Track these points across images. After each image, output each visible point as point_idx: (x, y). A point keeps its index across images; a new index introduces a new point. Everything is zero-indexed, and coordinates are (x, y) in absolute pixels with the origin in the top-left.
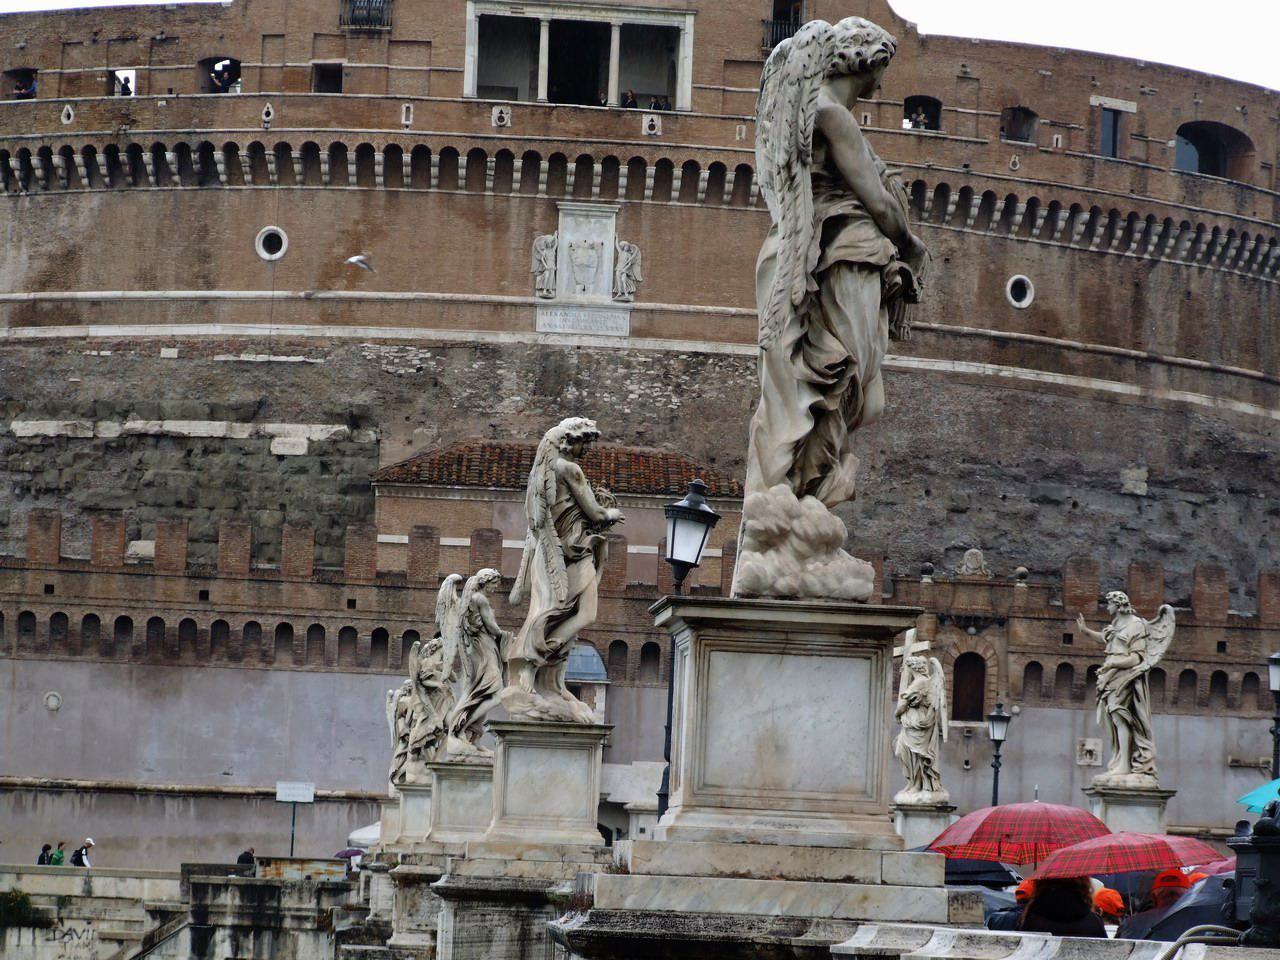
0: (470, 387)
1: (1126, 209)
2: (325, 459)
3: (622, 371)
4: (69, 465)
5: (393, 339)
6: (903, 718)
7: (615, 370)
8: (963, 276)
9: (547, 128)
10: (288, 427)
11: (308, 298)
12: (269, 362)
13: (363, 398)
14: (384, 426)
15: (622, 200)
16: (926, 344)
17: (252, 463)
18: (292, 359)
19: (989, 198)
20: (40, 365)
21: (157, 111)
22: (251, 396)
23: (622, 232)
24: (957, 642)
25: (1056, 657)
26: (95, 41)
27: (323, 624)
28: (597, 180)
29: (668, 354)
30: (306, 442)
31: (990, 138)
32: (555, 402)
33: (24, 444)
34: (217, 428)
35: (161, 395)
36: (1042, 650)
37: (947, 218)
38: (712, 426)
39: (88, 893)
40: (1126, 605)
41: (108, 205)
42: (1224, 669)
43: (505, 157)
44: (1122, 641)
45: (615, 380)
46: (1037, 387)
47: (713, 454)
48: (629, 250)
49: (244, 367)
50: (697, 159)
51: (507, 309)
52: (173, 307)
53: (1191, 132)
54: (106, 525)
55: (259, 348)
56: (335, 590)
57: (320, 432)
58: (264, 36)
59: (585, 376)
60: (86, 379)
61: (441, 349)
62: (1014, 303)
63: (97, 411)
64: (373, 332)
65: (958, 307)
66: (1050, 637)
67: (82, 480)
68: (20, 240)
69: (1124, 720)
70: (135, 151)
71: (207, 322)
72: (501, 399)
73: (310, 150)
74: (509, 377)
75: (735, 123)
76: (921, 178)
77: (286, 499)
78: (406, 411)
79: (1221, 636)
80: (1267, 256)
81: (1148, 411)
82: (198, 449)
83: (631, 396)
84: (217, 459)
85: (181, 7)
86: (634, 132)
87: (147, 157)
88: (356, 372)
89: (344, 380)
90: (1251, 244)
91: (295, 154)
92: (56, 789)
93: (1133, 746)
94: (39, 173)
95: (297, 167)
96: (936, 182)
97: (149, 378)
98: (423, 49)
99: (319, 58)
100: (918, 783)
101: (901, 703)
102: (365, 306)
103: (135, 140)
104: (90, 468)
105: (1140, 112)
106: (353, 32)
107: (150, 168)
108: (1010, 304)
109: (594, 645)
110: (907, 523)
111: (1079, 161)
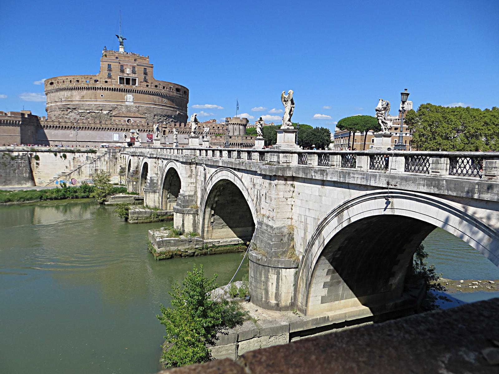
13: (111, 109)
22: (101, 109)
23: (132, 96)
24: (163, 129)
34: (98, 111)
39: (99, 150)
53: (176, 89)
57: (108, 112)
61: (117, 105)
81: (174, 111)
88: (110, 107)
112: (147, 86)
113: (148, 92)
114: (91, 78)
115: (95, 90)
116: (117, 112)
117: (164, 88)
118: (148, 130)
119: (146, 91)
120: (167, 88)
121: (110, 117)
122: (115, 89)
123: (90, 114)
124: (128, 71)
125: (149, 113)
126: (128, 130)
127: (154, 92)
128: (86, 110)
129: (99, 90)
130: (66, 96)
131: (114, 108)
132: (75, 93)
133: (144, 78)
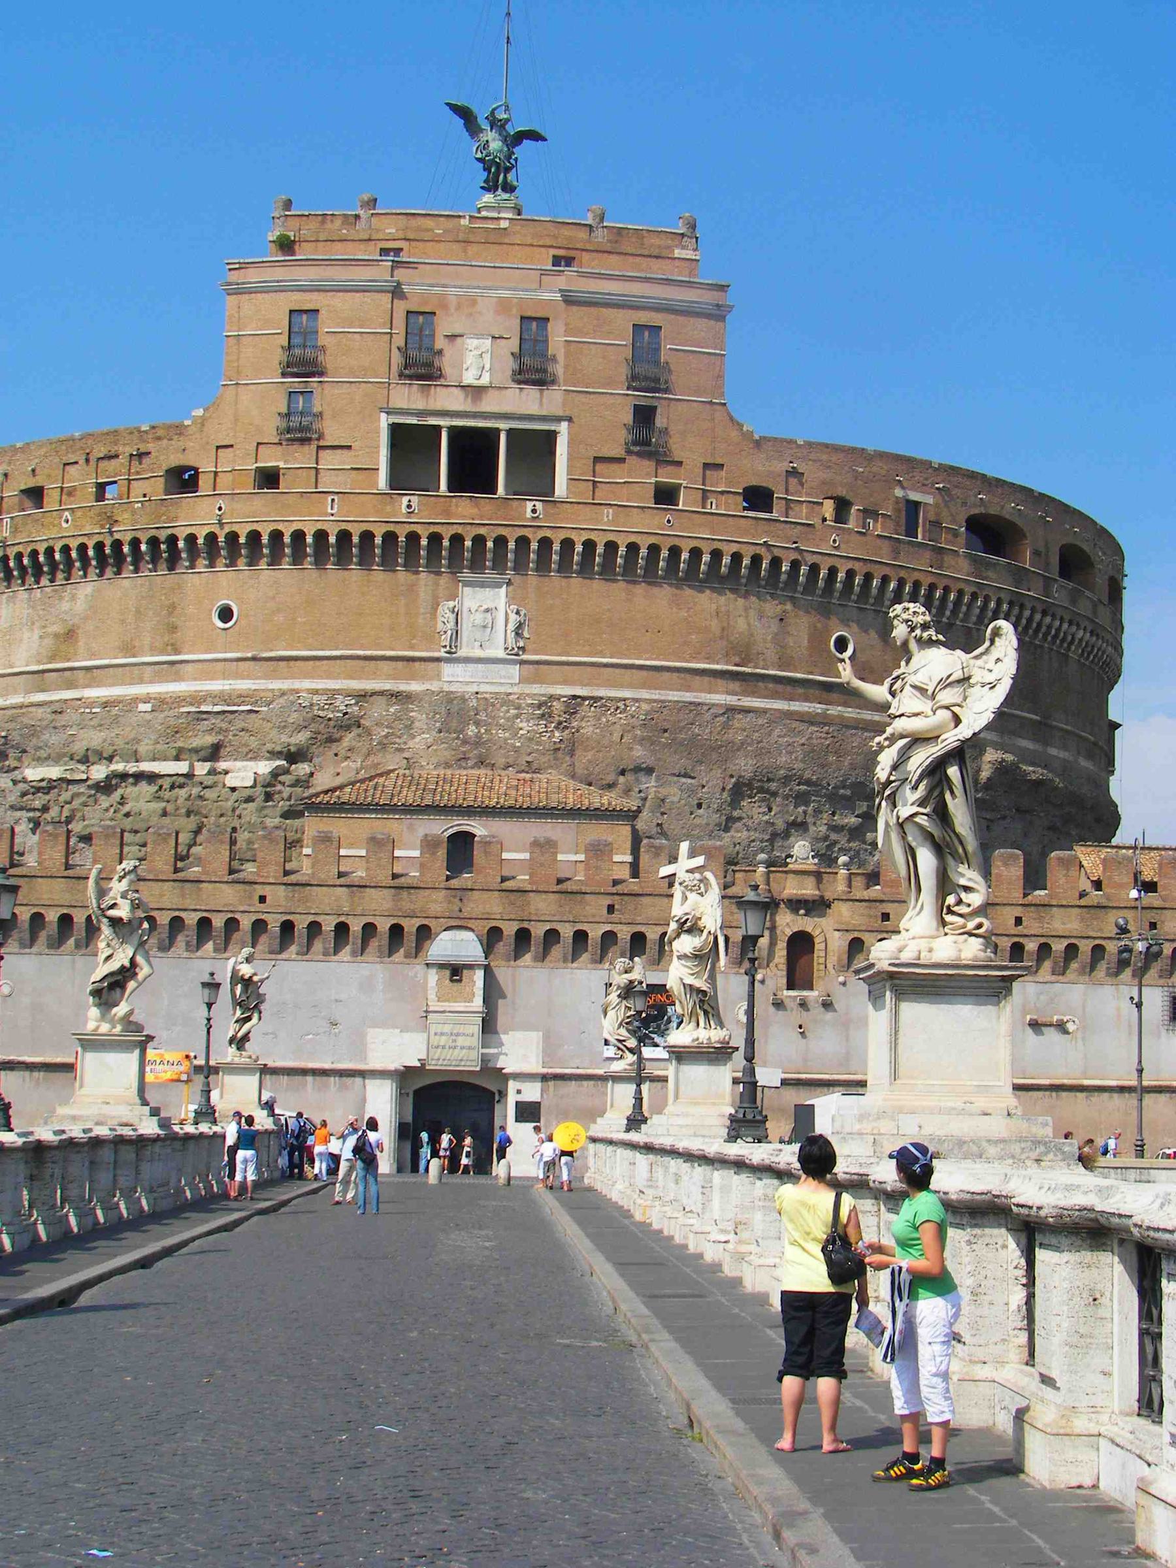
0: (387, 728)
1: (926, 581)
2: (268, 789)
4: (67, 803)
5: (323, 690)
6: (674, 944)
7: (508, 711)
9: (447, 513)
10: (239, 764)
11: (254, 659)
12: (224, 712)
13: (301, 738)
14: (316, 760)
17: (207, 793)
19: (814, 569)
20: (45, 723)
21: (134, 512)
22: (210, 739)
23: (510, 600)
25: (875, 934)
26: (87, 461)
27: (237, 916)
28: (489, 556)
29: (552, 696)
32: (458, 738)
33: (32, 787)
34: (182, 767)
35: (138, 741)
36: (864, 928)
37: (781, 585)
38: (590, 755)
40: (925, 627)
41: (99, 591)
42: (1021, 940)
43: (413, 537)
44: (922, 690)
45: (508, 719)
47: (590, 779)
48: (518, 613)
49: (204, 716)
50: (572, 537)
51: (417, 664)
52: (149, 669)
54: (50, 835)
55: (216, 701)
56: (247, 887)
57: (264, 767)
58: (218, 447)
59: (482, 716)
60: (81, 731)
64: (307, 684)
65: (792, 657)
66: (871, 917)
67: (79, 815)
68: (33, 624)
69: (929, 837)
71: (175, 681)
73: (254, 536)
74: (419, 717)
75: (603, 507)
76: (758, 552)
77: (236, 823)
78: (335, 747)
79: (1018, 912)
80: (1039, 625)
82: (166, 786)
83: (521, 732)
84: (183, 793)
85: (153, 428)
86: (522, 516)
87: (126, 549)
88: (294, 717)
89: (283, 724)
90: (1027, 613)
91: (242, 540)
93: (945, 885)
97: (130, 729)
98: (345, 452)
99: (261, 462)
100: (694, 1019)
101: (673, 926)
102: (299, 663)
103: (117, 536)
104: (85, 805)
105: (937, 505)
106: (288, 440)
107: (129, 559)
108: (835, 655)
109: (472, 930)
110: (754, 835)
111: (886, 542)
112: (665, 496)
113: (675, 551)
114: (141, 455)
115: (172, 567)
116: (349, 768)
117: (842, 506)
118: (624, 933)
121: (286, 815)
122: (344, 536)
123: (116, 795)
125: (683, 763)
126: (410, 939)
127: (737, 557)
128: (85, 760)
129: (202, 562)
133: (628, 418)
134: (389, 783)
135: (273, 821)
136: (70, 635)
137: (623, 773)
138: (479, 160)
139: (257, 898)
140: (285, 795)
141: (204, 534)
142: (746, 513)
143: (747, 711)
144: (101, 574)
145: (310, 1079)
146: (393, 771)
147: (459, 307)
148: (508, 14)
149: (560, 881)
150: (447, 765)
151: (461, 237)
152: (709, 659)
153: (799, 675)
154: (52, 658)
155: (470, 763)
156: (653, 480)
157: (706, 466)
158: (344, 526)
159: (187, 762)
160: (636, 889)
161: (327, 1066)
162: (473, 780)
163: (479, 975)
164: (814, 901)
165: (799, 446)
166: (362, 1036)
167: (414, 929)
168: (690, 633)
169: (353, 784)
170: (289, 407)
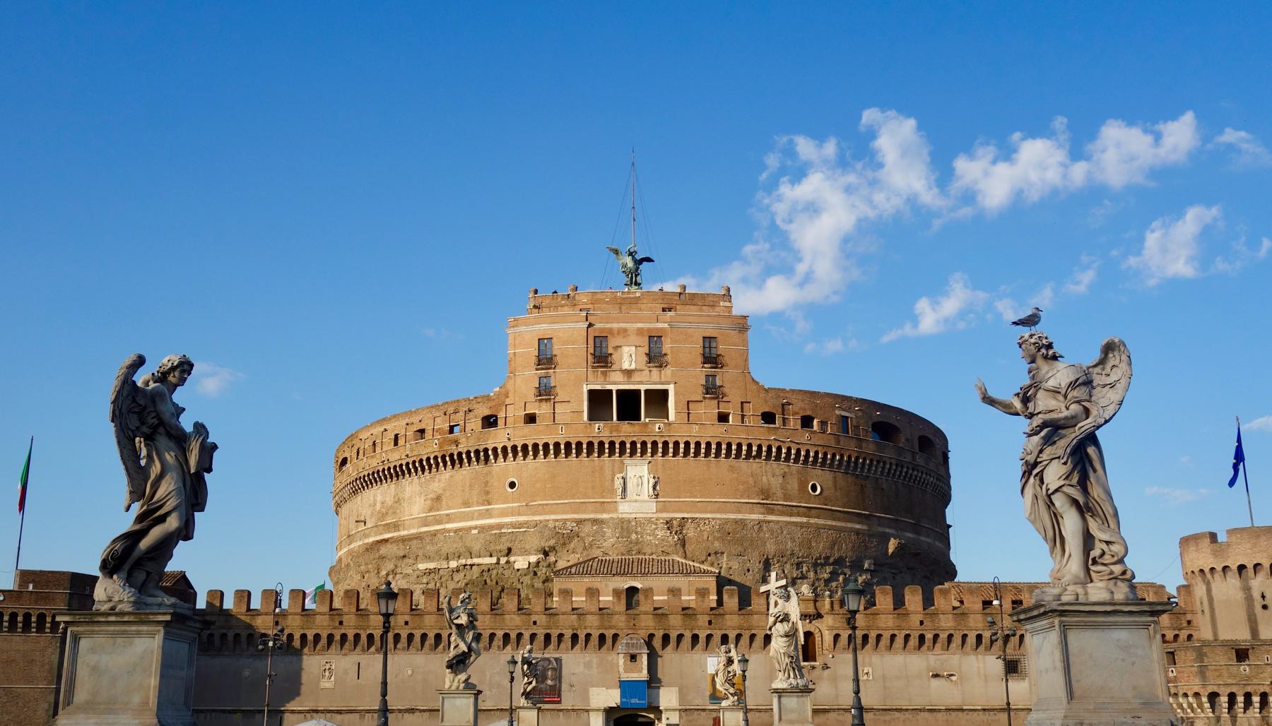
2: (535, 569)
3: (654, 526)
7: (651, 526)
8: (790, 482)
10: (520, 558)
14: (558, 555)
15: (650, 458)
16: (778, 510)
18: (521, 530)
26: (445, 414)
29: (672, 518)
30: (527, 563)
31: (799, 427)
32: (627, 541)
34: (494, 560)
41: (452, 476)
43: (601, 444)
46: (824, 526)
47: (693, 559)
48: (654, 478)
49: (504, 535)
51: (605, 504)
56: (527, 617)
57: (533, 559)
62: (812, 493)
63: (447, 559)
67: (444, 585)
70: (460, 454)
71: (488, 518)
72: (605, 541)
73: (525, 447)
74: (608, 531)
82: (486, 569)
84: (495, 572)
85: (475, 398)
87: (464, 456)
88: (547, 532)
91: (519, 449)
92: (412, 711)
94: (426, 467)
95: (520, 454)
96: (777, 445)
102: (549, 507)
112: (723, 418)
113: (729, 445)
116: (574, 559)
119: (719, 444)
120: (823, 423)
121: (544, 582)
122: (568, 445)
123: (462, 575)
124: (629, 356)
126: (609, 641)
127: (760, 447)
128: (447, 559)
130: (378, 507)
131: (565, 538)
132: (411, 486)
133: (704, 384)
134: (595, 564)
135: (538, 584)
136: (438, 498)
137: (709, 555)
138: (623, 272)
139: (532, 624)
140: (544, 572)
141: (501, 446)
142: (763, 425)
143: (769, 522)
144: (453, 468)
145: (561, 714)
146: (597, 558)
147: (618, 334)
148: (634, 208)
149: (684, 609)
150: (623, 554)
151: (619, 301)
152: (749, 497)
153: (795, 504)
154: (431, 510)
155: (634, 553)
156: (717, 411)
157: (742, 403)
158: (568, 440)
159: (496, 558)
160: (722, 611)
161: (569, 708)
162: (636, 561)
163: (645, 658)
164: (814, 616)
165: (787, 392)
166: (587, 692)
167: (611, 636)
168: (738, 485)
169: (576, 565)
170: (540, 384)
